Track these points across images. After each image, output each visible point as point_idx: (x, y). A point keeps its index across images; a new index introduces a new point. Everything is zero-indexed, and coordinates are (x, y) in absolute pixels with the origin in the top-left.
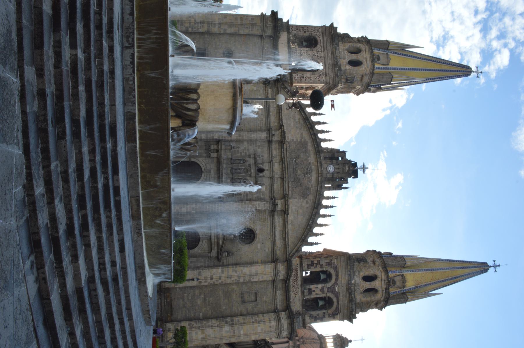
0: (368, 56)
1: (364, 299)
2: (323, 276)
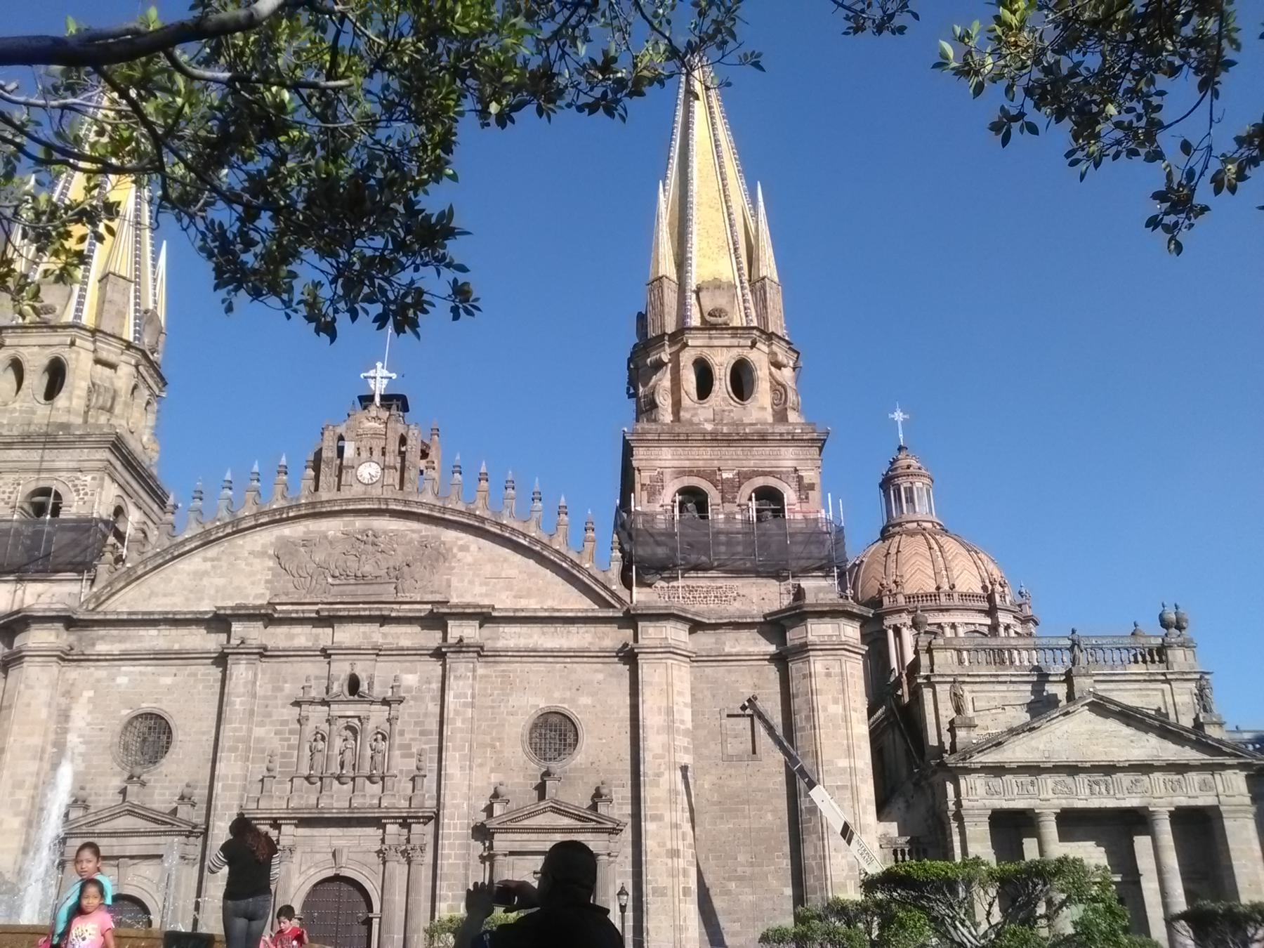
0: (34, 338)
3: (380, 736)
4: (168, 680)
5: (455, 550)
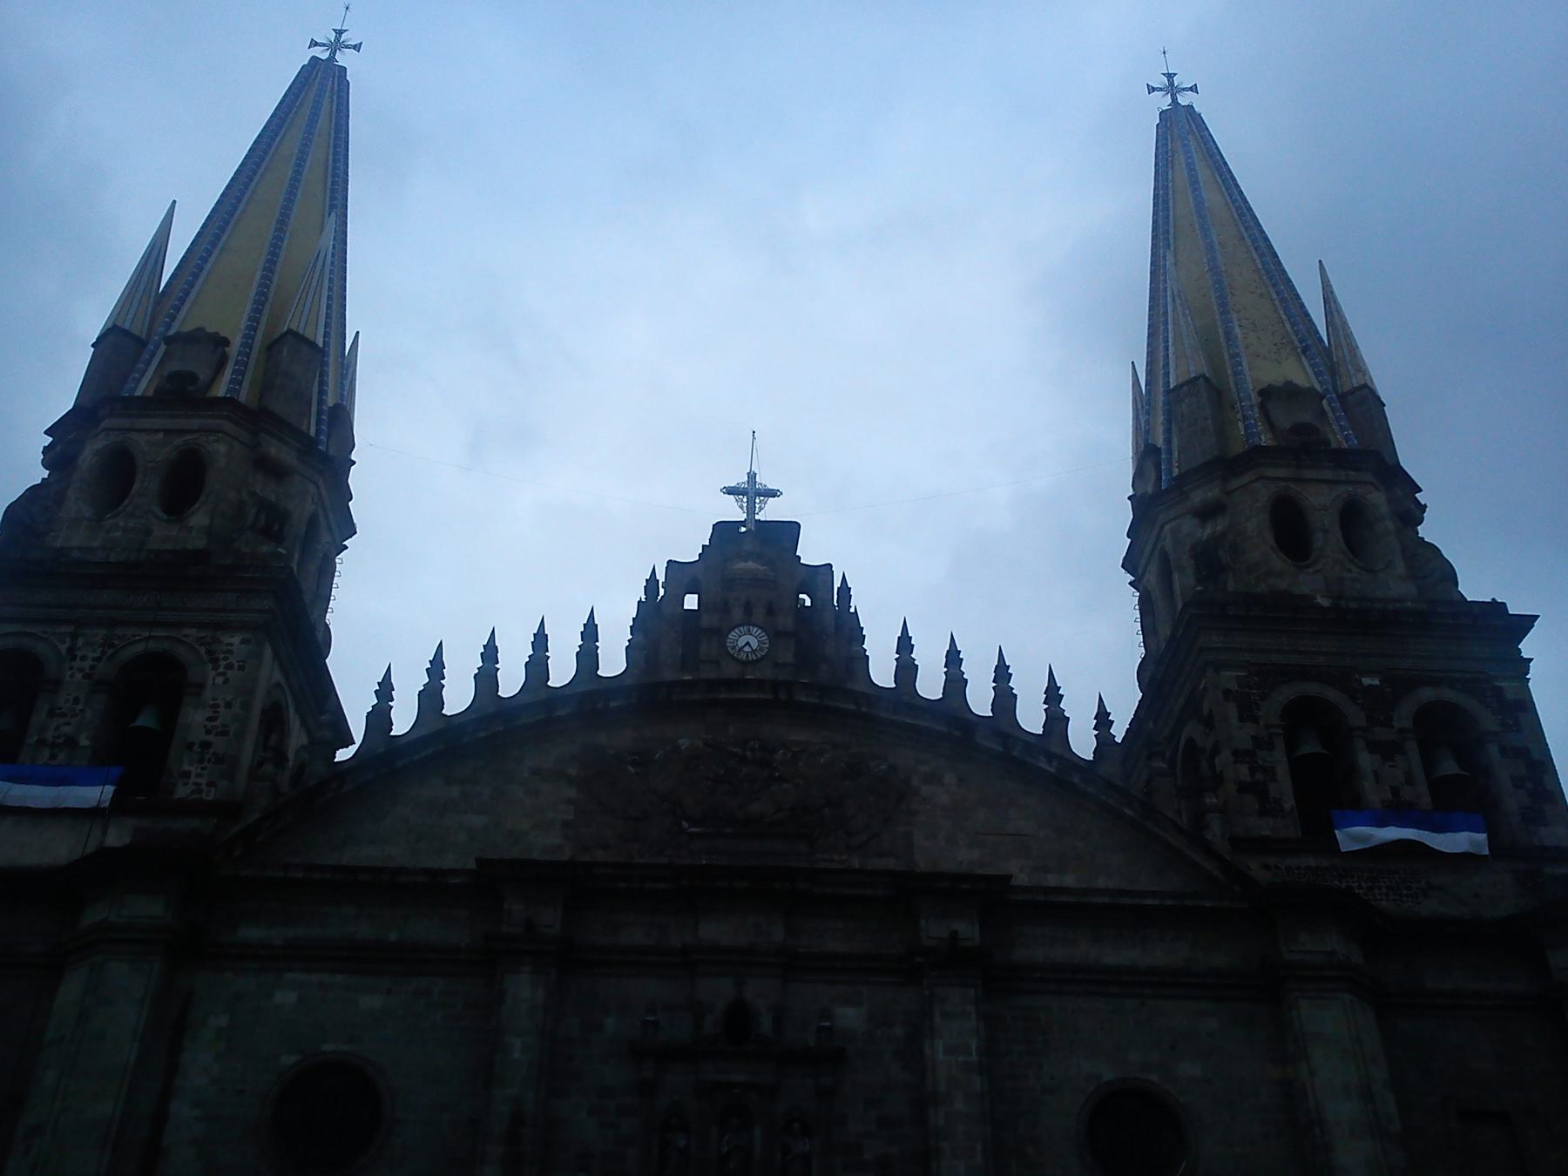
1: (1400, 567)
2: (1310, 746)
3: (797, 1125)
4: (371, 1002)
5: (915, 782)
